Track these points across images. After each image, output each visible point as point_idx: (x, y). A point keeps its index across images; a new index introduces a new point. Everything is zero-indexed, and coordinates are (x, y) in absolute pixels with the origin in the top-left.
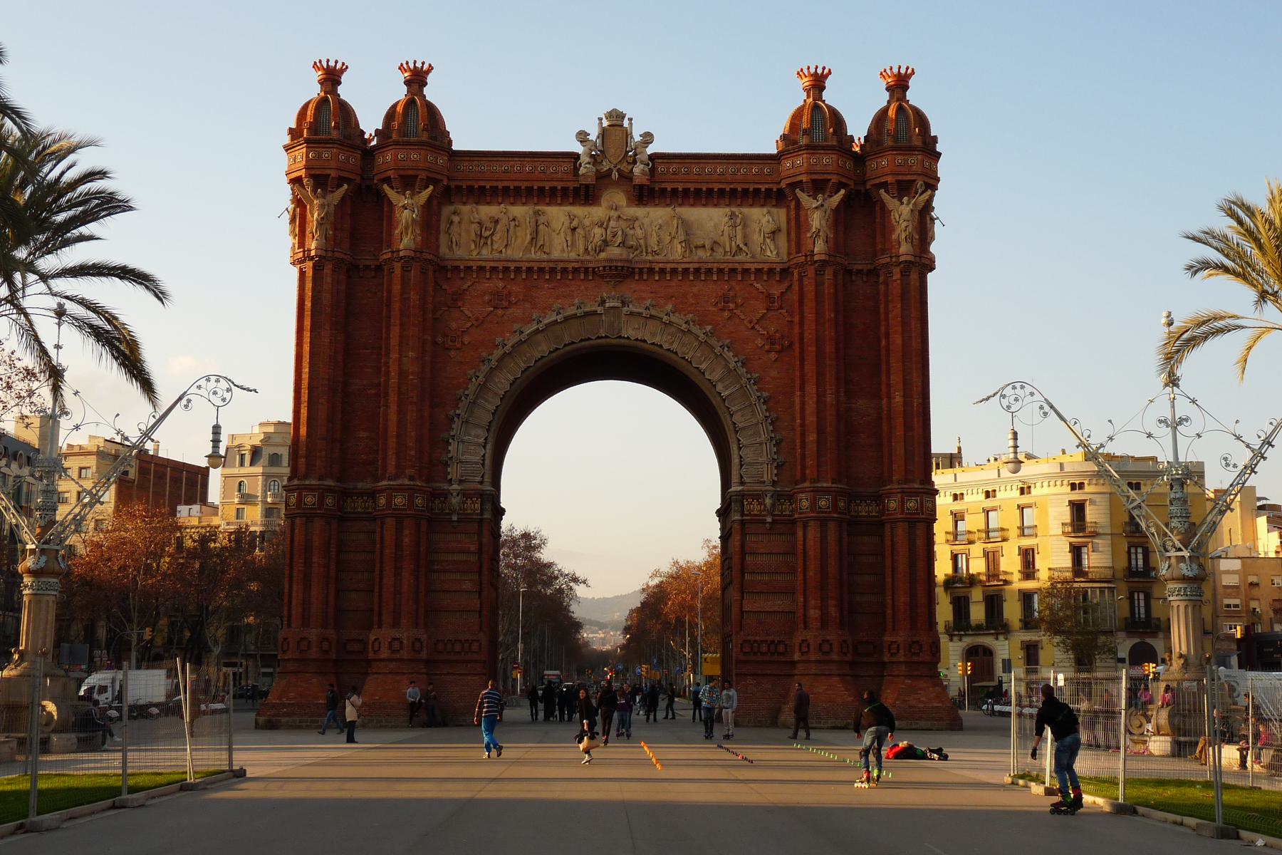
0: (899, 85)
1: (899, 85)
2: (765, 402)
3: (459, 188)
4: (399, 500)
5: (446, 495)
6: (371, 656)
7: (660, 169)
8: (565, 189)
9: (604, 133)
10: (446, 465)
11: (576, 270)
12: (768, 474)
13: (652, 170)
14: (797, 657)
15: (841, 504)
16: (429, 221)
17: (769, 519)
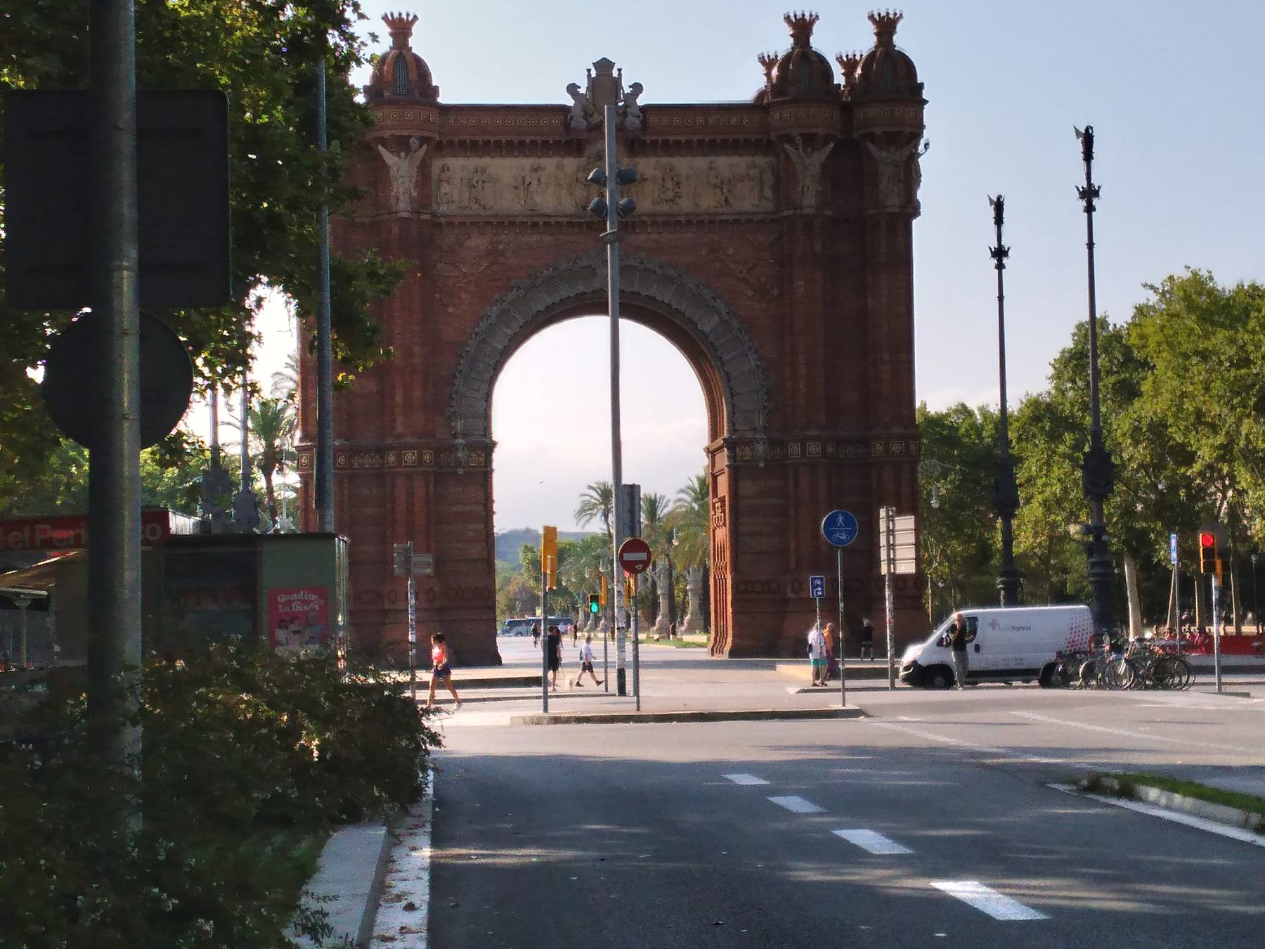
0: (886, 26)
1: (886, 26)
2: (756, 351)
3: (451, 143)
4: (410, 457)
5: (453, 448)
6: (386, 607)
7: (653, 120)
8: (557, 143)
9: (593, 83)
10: (449, 419)
11: (570, 224)
12: (760, 421)
13: (644, 123)
14: (790, 595)
15: (830, 449)
16: (424, 175)
17: (762, 465)
